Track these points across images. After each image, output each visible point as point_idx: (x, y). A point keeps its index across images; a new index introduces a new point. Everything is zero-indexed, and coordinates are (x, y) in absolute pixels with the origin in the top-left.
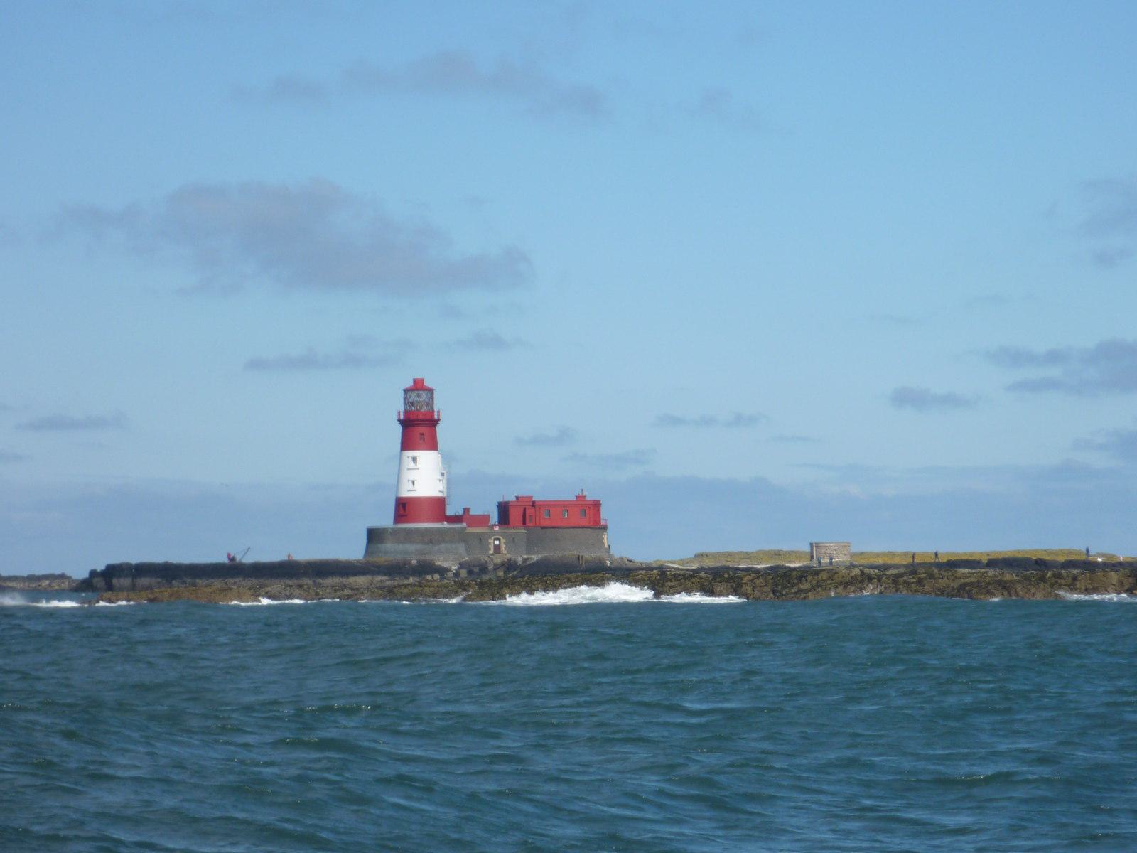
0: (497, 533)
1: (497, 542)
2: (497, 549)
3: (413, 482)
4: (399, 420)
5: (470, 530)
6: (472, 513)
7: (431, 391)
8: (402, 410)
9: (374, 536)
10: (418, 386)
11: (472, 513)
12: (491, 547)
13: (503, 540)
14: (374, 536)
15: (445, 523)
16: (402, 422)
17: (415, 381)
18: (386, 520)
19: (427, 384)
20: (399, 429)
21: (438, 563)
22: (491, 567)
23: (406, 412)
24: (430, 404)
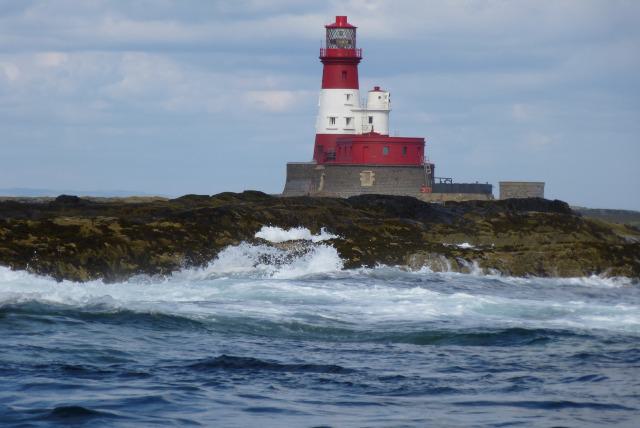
4: (321, 58)
7: (354, 28)
8: (324, 47)
9: (294, 171)
10: (342, 22)
14: (294, 171)
16: (324, 60)
19: (350, 21)
20: (321, 66)
23: (328, 50)
24: (352, 41)
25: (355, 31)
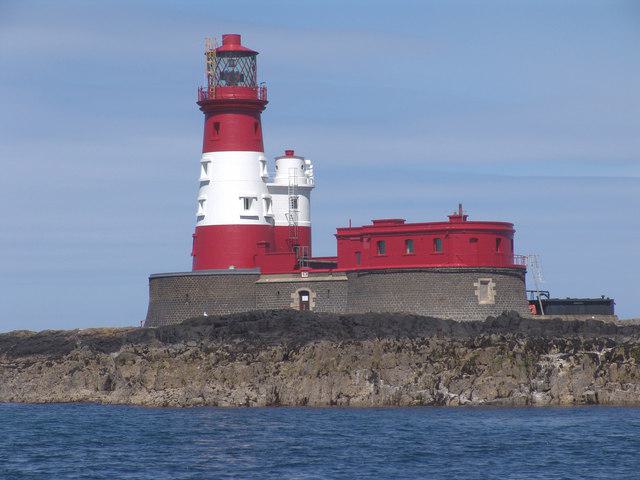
7: (252, 54)
8: (205, 85)
10: (232, 50)
13: (313, 295)
17: (226, 39)
18: (180, 260)
19: (246, 44)
20: (202, 116)
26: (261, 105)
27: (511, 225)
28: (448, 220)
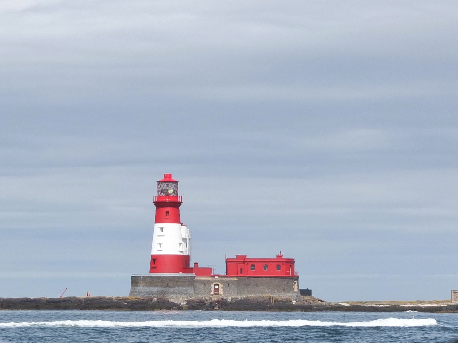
0: (218, 281)
1: (217, 287)
2: (217, 291)
3: (161, 244)
4: (154, 202)
5: (197, 278)
6: (200, 266)
7: (177, 182)
9: (135, 280)
10: (168, 180)
11: (200, 266)
12: (213, 290)
13: (221, 286)
14: (135, 280)
15: (181, 273)
16: (156, 203)
17: (166, 176)
18: (144, 270)
19: (174, 178)
20: (155, 207)
21: (171, 300)
22: (208, 304)
24: (176, 191)
25: (177, 185)
26: (179, 204)
27: (294, 259)
28: (276, 258)
